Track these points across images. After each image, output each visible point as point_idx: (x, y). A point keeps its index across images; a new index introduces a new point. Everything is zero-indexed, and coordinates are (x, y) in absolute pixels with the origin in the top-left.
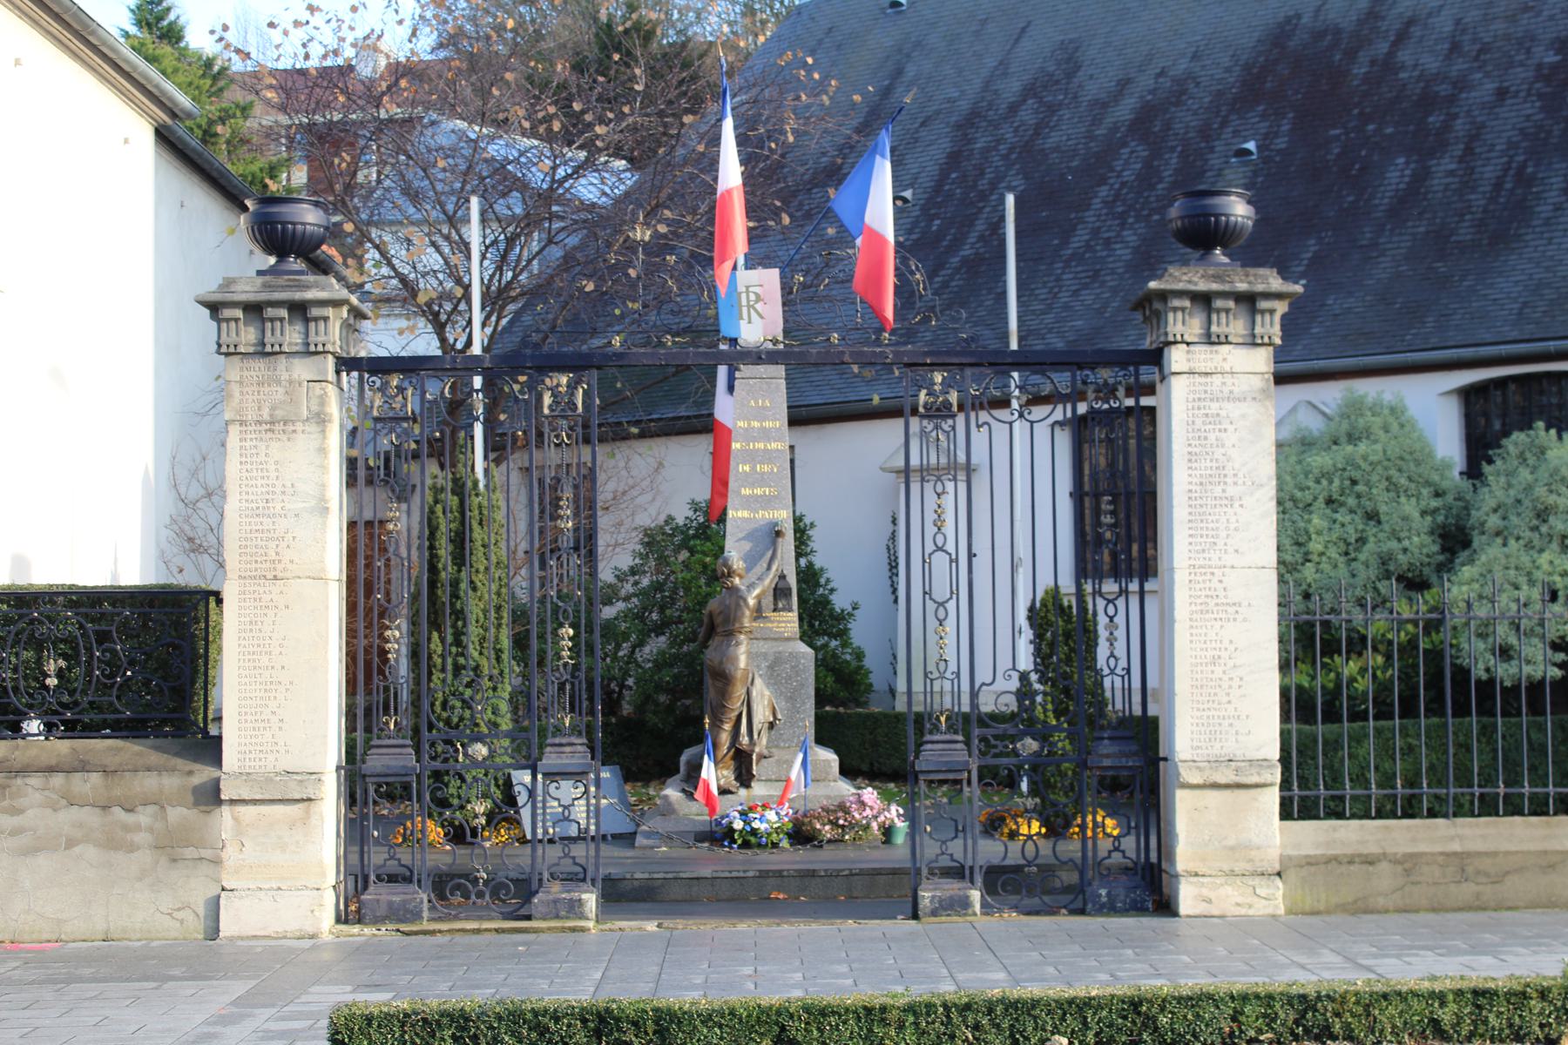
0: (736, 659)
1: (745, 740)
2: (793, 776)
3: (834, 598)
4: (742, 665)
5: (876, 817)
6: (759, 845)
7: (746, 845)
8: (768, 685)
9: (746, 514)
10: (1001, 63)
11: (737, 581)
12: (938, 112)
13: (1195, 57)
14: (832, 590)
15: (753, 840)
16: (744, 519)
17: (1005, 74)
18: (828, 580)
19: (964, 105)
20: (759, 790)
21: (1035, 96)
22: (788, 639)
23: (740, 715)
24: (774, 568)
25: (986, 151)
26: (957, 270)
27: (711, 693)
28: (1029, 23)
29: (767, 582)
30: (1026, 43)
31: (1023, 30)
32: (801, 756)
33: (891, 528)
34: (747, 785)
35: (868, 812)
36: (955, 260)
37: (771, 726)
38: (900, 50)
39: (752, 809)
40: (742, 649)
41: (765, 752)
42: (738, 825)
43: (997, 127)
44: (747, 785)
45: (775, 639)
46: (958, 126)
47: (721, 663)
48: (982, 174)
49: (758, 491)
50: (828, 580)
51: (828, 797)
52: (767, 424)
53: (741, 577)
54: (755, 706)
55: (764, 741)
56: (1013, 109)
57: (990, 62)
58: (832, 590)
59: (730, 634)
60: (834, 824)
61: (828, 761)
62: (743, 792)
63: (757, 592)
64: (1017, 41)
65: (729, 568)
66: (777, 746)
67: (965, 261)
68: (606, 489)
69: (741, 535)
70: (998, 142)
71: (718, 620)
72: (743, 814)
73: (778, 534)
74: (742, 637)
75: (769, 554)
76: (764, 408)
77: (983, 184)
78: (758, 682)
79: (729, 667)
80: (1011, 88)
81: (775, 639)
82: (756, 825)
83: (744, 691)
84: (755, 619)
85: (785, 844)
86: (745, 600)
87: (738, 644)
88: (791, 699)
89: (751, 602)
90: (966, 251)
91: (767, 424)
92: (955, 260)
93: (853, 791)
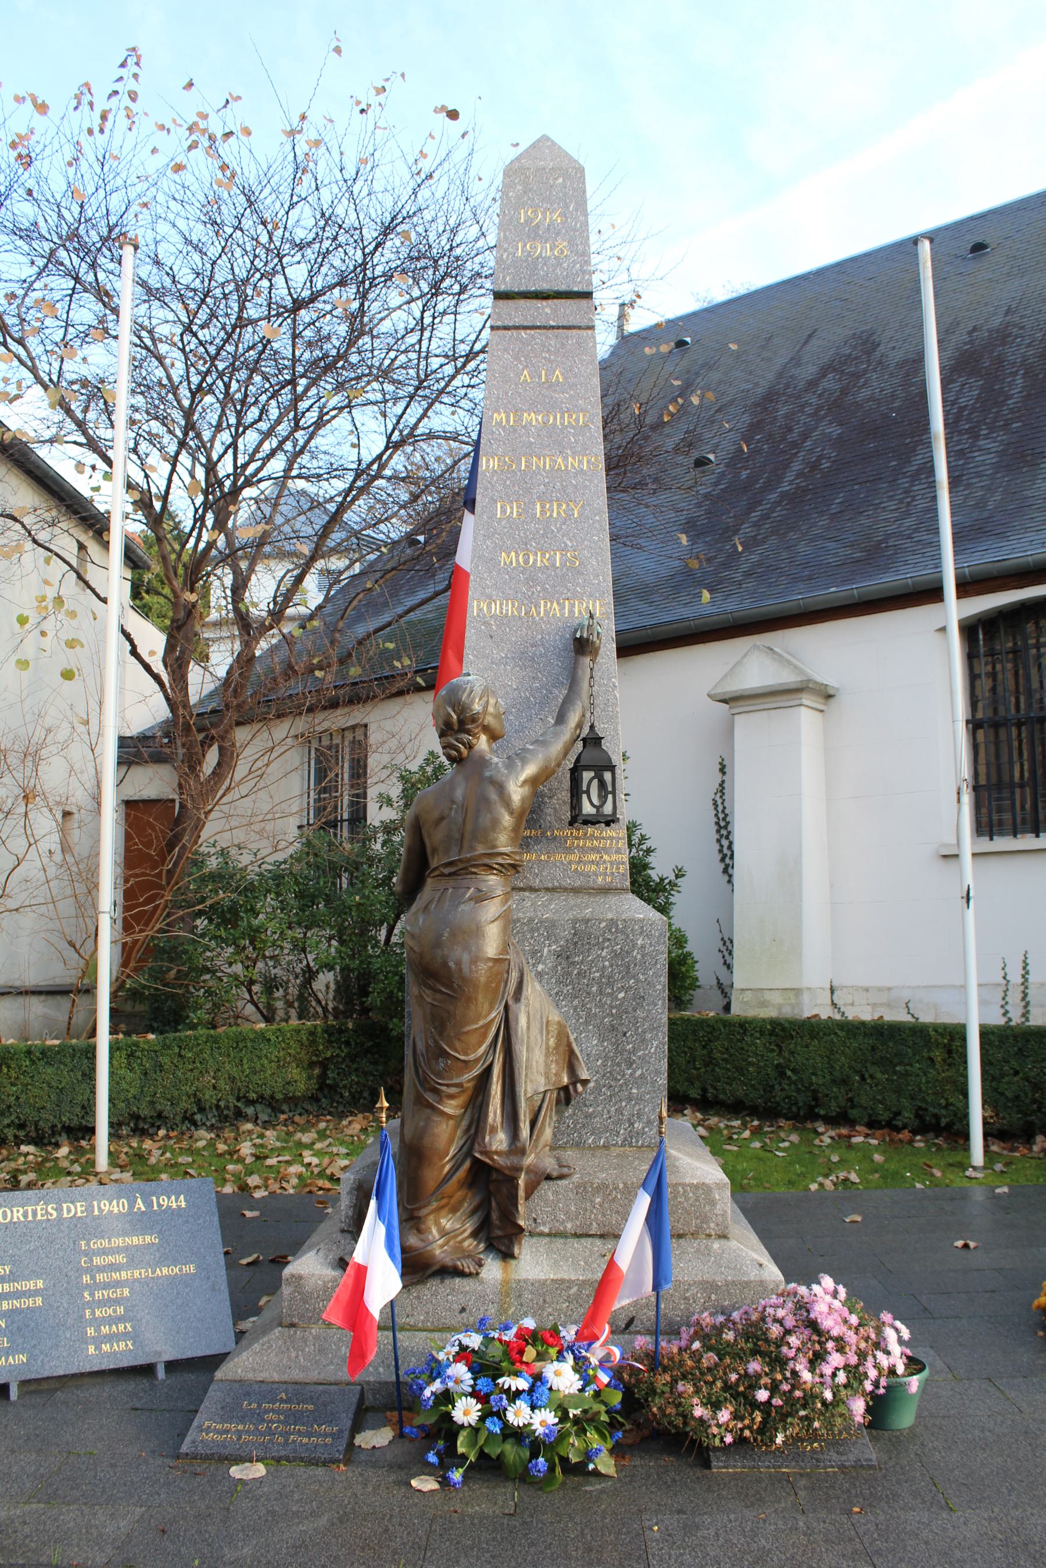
0: (477, 932)
1: (499, 1141)
2: (624, 1260)
3: (651, 859)
4: (491, 948)
5: (855, 1373)
6: (524, 1477)
7: (488, 1467)
8: (557, 998)
9: (509, 609)
10: (792, 359)
11: (482, 743)
12: (733, 401)
13: (1008, 312)
14: (649, 851)
15: (511, 1451)
16: (503, 620)
17: (798, 365)
18: (643, 838)
19: (759, 391)
20: (533, 1263)
21: (835, 370)
22: (605, 891)
23: (488, 1071)
24: (573, 719)
25: (790, 416)
26: (778, 503)
27: (415, 1027)
28: (815, 331)
29: (556, 748)
30: (814, 341)
31: (810, 336)
32: (643, 1202)
33: (719, 777)
34: (507, 1256)
35: (836, 1359)
36: (773, 497)
37: (565, 1096)
38: (688, 372)
39: (513, 1356)
40: (492, 909)
41: (549, 1164)
42: (466, 1411)
43: (799, 397)
44: (507, 1256)
45: (576, 891)
46: (756, 405)
47: (438, 944)
48: (790, 430)
49: (538, 560)
50: (643, 838)
51: (710, 1287)
52: (556, 419)
53: (493, 737)
54: (522, 1053)
55: (548, 1133)
56: (812, 384)
57: (780, 361)
58: (649, 851)
59: (462, 870)
60: (741, 1395)
61: (704, 1189)
62: (492, 1270)
63: (530, 770)
64: (806, 343)
65: (461, 708)
66: (578, 1145)
67: (784, 495)
68: (374, 737)
69: (498, 654)
70: (803, 406)
71: (435, 837)
72: (483, 1367)
73: (582, 646)
74: (493, 881)
75: (561, 694)
76: (550, 385)
77: (794, 436)
78: (533, 990)
79: (458, 956)
80: (808, 371)
81: (576, 891)
82: (519, 1414)
83: (496, 1014)
84: (525, 844)
85: (605, 1464)
86: (501, 789)
87: (481, 897)
88: (613, 1032)
89: (517, 793)
90: (785, 487)
91: (556, 419)
92: (773, 497)
93: (773, 1273)
